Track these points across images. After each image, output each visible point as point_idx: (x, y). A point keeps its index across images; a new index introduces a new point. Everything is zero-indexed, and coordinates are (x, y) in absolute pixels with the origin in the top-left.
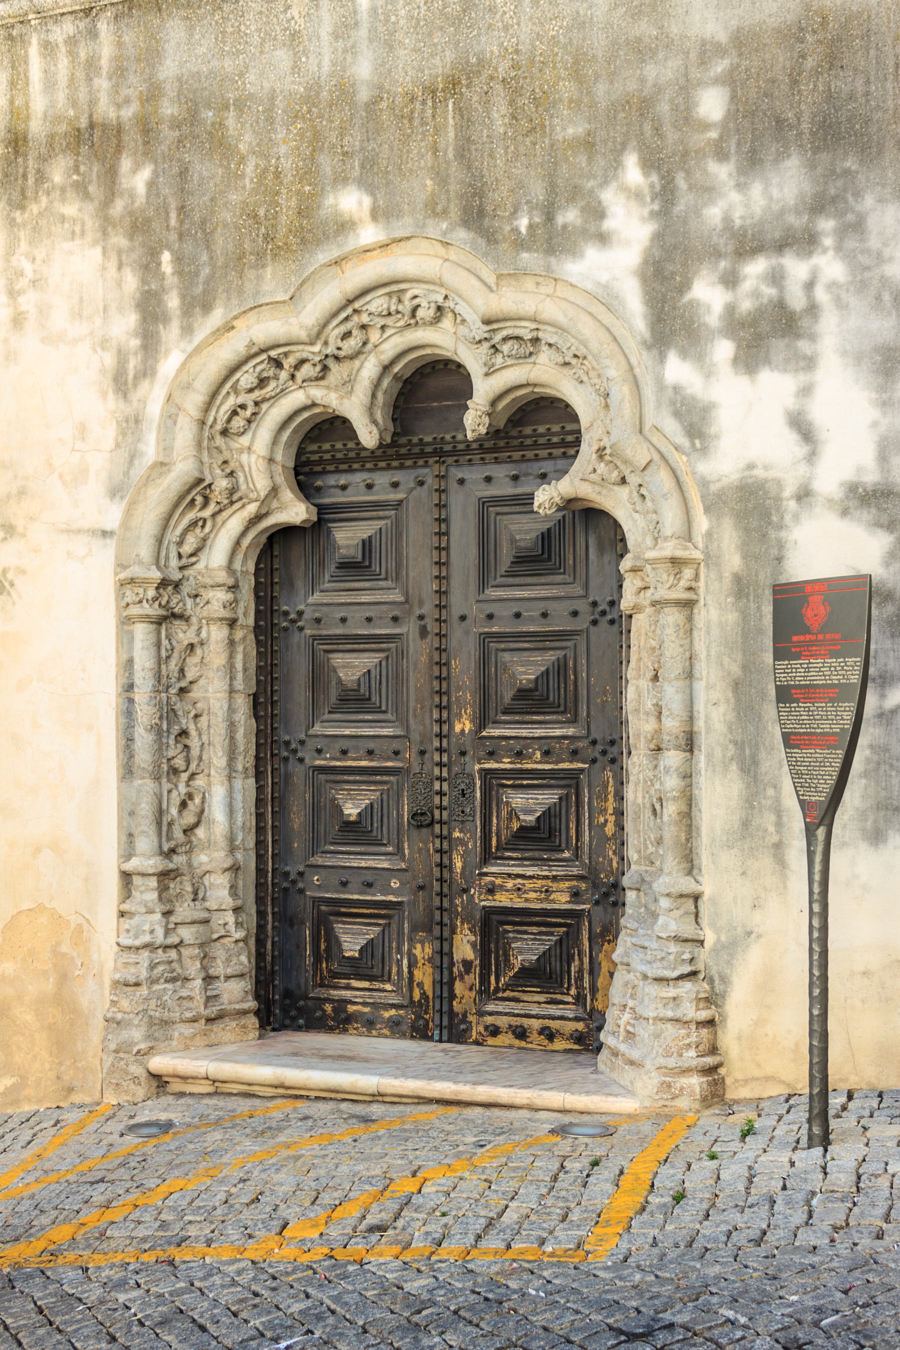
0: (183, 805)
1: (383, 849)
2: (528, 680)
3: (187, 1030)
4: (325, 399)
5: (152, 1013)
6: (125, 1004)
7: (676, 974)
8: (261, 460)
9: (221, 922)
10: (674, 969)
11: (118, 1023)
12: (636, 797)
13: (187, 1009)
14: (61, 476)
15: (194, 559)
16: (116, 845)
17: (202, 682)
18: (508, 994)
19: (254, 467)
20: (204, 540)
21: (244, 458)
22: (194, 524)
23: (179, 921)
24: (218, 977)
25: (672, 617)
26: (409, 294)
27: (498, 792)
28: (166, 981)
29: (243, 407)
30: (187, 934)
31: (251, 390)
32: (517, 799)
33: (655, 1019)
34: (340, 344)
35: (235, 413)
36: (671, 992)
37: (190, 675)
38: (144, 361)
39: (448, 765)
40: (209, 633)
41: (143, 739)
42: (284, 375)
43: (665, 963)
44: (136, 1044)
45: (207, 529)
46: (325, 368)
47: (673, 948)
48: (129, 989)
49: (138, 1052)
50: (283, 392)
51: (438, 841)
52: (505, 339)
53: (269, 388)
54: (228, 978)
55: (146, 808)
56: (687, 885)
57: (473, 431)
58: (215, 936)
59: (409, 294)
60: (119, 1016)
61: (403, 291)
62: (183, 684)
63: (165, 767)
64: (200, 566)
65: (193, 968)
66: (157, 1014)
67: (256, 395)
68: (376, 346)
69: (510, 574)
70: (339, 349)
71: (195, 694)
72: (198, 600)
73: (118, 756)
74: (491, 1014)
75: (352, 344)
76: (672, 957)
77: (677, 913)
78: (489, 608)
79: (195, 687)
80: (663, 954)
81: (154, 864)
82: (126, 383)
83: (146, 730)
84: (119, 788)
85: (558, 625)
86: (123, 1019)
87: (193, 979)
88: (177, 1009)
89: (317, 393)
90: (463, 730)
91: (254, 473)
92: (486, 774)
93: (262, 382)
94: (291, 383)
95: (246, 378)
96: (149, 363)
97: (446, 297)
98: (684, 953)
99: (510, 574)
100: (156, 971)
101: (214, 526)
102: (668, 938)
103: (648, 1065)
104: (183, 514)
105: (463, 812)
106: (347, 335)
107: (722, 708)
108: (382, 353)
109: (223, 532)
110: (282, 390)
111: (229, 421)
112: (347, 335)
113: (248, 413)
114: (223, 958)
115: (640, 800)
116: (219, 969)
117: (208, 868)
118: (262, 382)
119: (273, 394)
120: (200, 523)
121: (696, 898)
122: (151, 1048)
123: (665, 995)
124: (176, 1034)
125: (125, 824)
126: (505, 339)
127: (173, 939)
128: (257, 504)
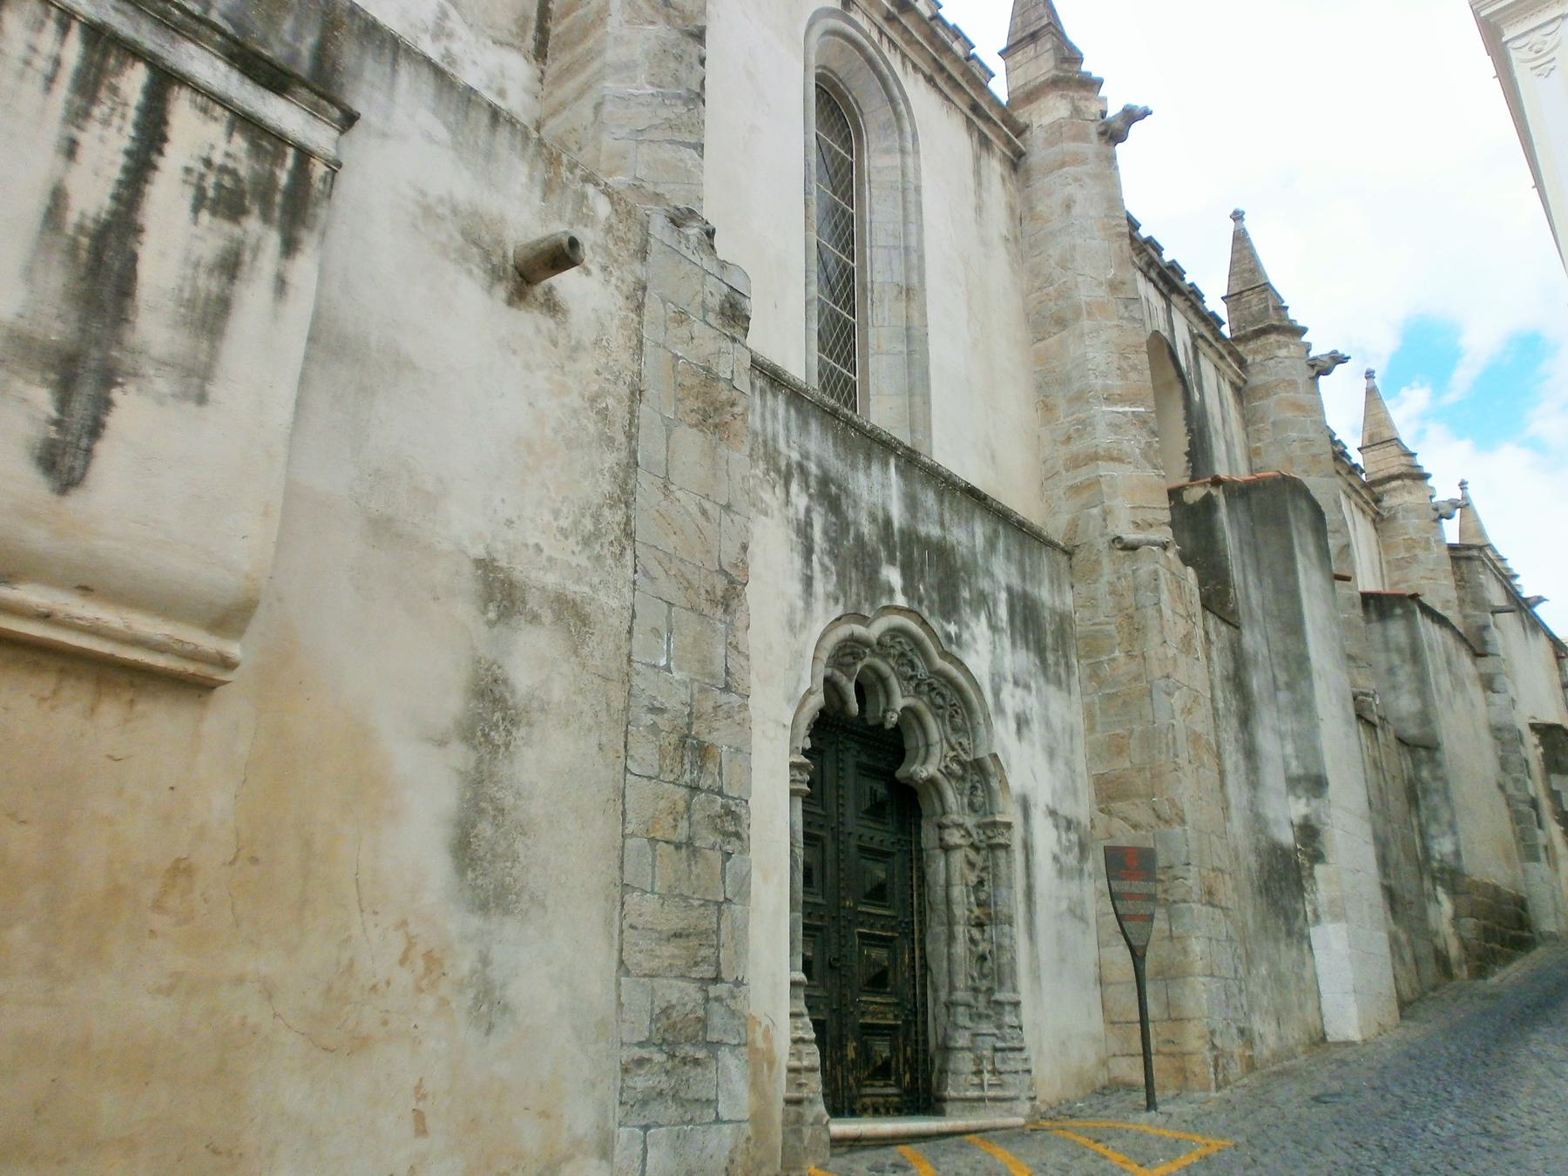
18: (868, 1082)
61: (898, 637)
74: (866, 1096)
103: (1023, 1097)
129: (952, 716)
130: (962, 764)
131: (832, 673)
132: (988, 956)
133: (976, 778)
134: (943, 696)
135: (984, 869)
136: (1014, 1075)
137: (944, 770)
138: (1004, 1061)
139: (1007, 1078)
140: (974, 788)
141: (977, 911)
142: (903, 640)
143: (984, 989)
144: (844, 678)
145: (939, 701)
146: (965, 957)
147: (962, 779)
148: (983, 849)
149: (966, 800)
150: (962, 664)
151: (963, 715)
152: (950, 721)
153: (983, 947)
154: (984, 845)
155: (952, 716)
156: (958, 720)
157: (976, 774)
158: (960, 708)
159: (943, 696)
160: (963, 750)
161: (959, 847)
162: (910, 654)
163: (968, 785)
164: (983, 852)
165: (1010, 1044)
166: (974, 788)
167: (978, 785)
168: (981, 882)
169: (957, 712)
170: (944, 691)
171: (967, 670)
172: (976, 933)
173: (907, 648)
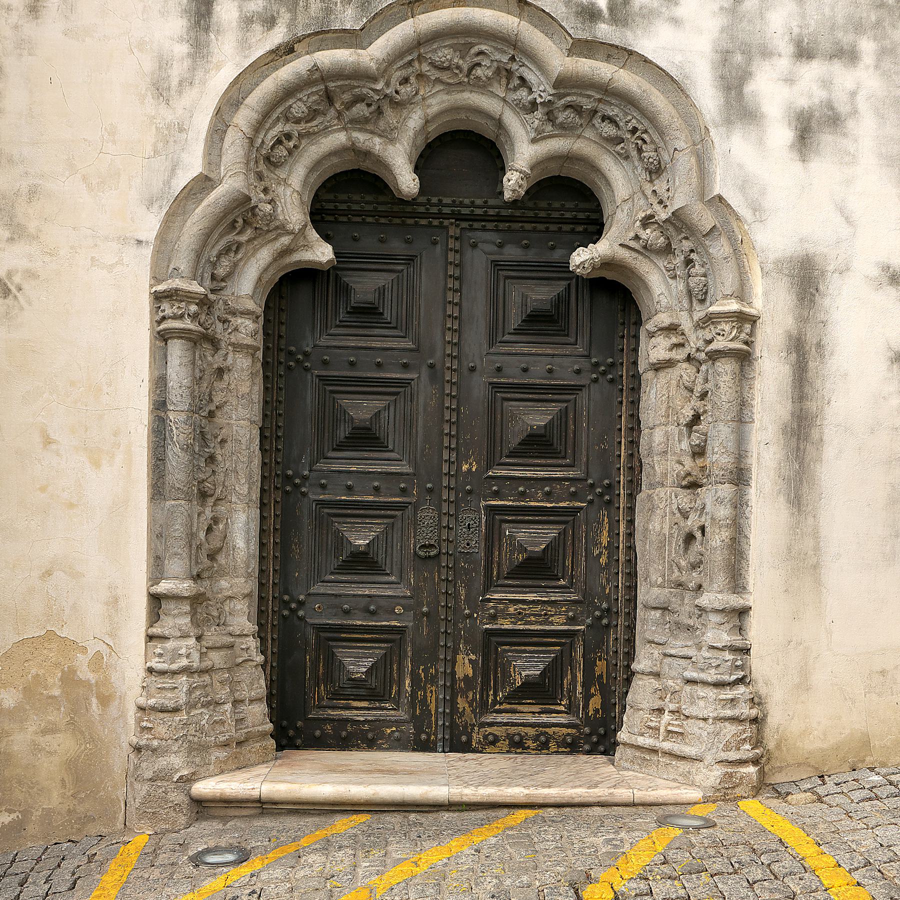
0: (209, 530)
1: (386, 579)
2: (538, 426)
3: (222, 754)
4: (367, 143)
5: (191, 738)
6: (161, 730)
7: (733, 678)
8: (295, 194)
9: (243, 647)
10: (731, 674)
11: (154, 750)
12: (662, 528)
13: (220, 733)
14: (85, 178)
15: (224, 284)
16: (144, 567)
17: (226, 409)
19: (289, 200)
20: (235, 265)
21: (281, 189)
22: (227, 250)
23: (210, 644)
24: (242, 701)
25: (726, 367)
26: (475, 50)
27: (500, 527)
28: (203, 706)
29: (288, 137)
30: (216, 658)
31: (298, 121)
32: (523, 534)
33: (715, 719)
34: (399, 88)
35: (279, 142)
36: (728, 694)
37: (218, 399)
38: (193, 69)
39: (456, 502)
40: (235, 360)
41: (176, 457)
42: (332, 113)
43: (721, 670)
44: (177, 770)
45: (239, 256)
46: (379, 112)
47: (728, 656)
48: (165, 715)
49: (181, 777)
50: (325, 131)
51: (444, 571)
52: (568, 106)
53: (315, 123)
54: (251, 701)
55: (178, 528)
56: (735, 601)
57: (514, 191)
58: (240, 660)
59: (475, 50)
60: (155, 743)
61: (472, 45)
62: (212, 407)
63: (195, 489)
64: (228, 292)
65: (223, 693)
66: (196, 739)
67: (302, 126)
68: (424, 99)
69: (517, 332)
70: (397, 92)
71: (220, 420)
72: (226, 326)
73: (148, 476)
75: (407, 90)
76: (729, 663)
77: (727, 626)
78: (499, 361)
79: (219, 414)
80: (718, 662)
81: (185, 587)
82: (169, 89)
83: (182, 449)
84: (148, 508)
85: (563, 380)
86: (160, 746)
87: (224, 703)
88: (212, 733)
89: (361, 138)
90: (470, 470)
91: (289, 206)
92: (492, 510)
93: (313, 114)
94: (336, 122)
95: (298, 108)
96: (199, 74)
97: (513, 59)
98: (737, 660)
99: (517, 332)
100: (193, 696)
101: (246, 254)
102: (722, 649)
104: (221, 236)
105: (468, 544)
106: (405, 81)
107: (773, 448)
108: (429, 106)
109: (253, 260)
110: (326, 128)
111: (272, 148)
112: (405, 81)
113: (291, 144)
114: (248, 682)
115: (666, 531)
116: (245, 693)
117: (229, 593)
118: (313, 114)
119: (316, 129)
120: (234, 248)
121: (743, 612)
122: (193, 774)
123: (724, 697)
124: (213, 758)
125: (153, 546)
126: (568, 106)
127: (207, 664)
128: (291, 237)
129: (640, 151)
130: (662, 227)
131: (349, 138)
132: (698, 535)
133: (687, 245)
134: (612, 120)
135: (703, 396)
136: (701, 724)
137: (632, 244)
138: (693, 702)
139: (692, 727)
140: (688, 262)
141: (688, 462)
142: (483, 48)
143: (692, 585)
144: (377, 140)
145: (609, 130)
146: (671, 535)
147: (667, 250)
148: (705, 361)
149: (681, 286)
150: (631, 53)
151: (653, 142)
152: (641, 159)
153: (693, 522)
154: (702, 356)
155: (640, 151)
156: (649, 152)
157: (686, 238)
158: (646, 132)
159: (612, 120)
160: (661, 202)
161: (669, 364)
162: (515, 67)
163: (679, 260)
164: (703, 368)
165: (703, 676)
166: (688, 262)
167: (693, 256)
168: (696, 419)
169: (645, 142)
170: (611, 111)
171: (646, 61)
172: (684, 499)
173: (505, 59)
